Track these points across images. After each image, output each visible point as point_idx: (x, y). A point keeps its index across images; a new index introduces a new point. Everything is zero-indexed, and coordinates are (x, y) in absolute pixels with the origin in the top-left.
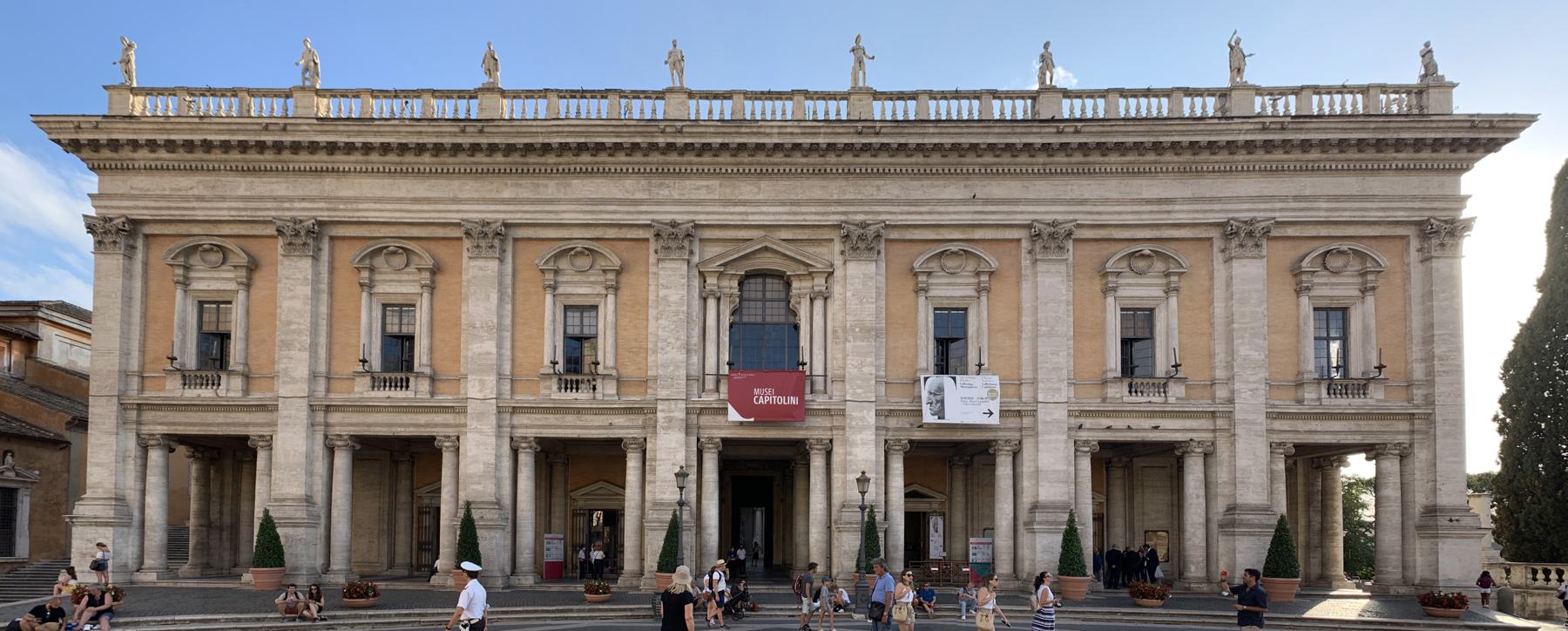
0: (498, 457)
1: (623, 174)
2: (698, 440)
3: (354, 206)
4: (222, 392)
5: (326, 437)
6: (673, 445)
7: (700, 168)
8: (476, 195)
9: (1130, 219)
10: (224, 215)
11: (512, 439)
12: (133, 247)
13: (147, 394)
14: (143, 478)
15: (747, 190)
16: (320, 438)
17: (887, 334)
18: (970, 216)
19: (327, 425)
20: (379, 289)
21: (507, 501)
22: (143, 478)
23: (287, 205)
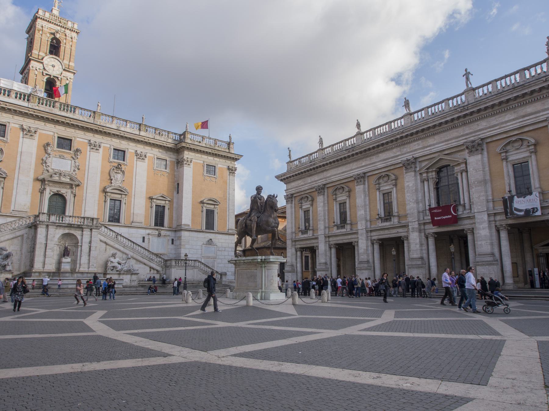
0: (367, 246)
1: (392, 148)
2: (425, 234)
3: (330, 178)
4: (308, 235)
5: (329, 245)
6: (415, 238)
7: (414, 139)
8: (356, 167)
10: (306, 188)
11: (371, 240)
12: (292, 201)
13: (296, 237)
14: (296, 259)
15: (431, 141)
16: (328, 245)
17: (491, 181)
19: (329, 241)
20: (338, 200)
21: (371, 261)
22: (296, 259)
23: (317, 182)
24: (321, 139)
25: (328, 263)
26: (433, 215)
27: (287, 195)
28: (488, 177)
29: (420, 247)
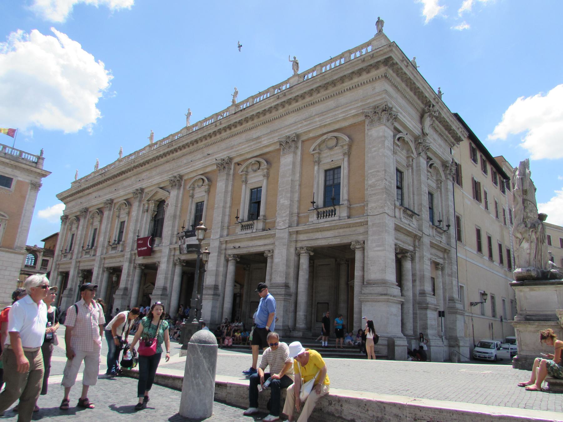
9: (248, 150)
16: (77, 270)
17: (180, 217)
18: (202, 165)
24: (98, 162)
25: (73, 289)
26: (139, 246)
27: (63, 216)
28: (178, 213)
29: (127, 277)
